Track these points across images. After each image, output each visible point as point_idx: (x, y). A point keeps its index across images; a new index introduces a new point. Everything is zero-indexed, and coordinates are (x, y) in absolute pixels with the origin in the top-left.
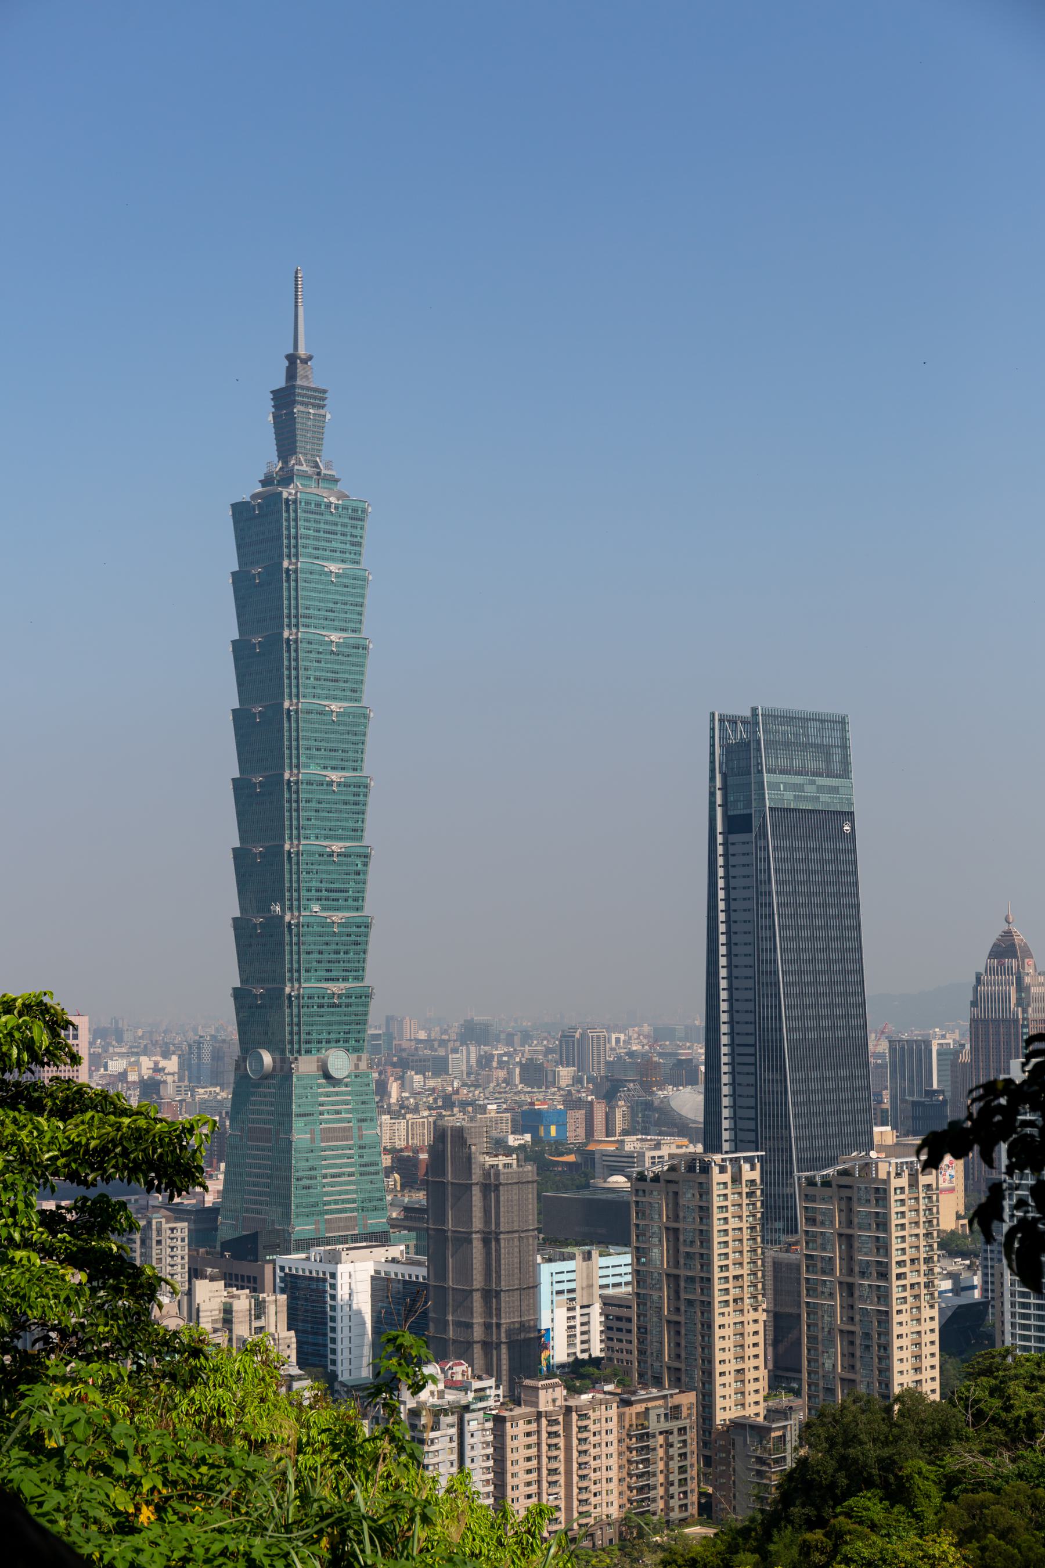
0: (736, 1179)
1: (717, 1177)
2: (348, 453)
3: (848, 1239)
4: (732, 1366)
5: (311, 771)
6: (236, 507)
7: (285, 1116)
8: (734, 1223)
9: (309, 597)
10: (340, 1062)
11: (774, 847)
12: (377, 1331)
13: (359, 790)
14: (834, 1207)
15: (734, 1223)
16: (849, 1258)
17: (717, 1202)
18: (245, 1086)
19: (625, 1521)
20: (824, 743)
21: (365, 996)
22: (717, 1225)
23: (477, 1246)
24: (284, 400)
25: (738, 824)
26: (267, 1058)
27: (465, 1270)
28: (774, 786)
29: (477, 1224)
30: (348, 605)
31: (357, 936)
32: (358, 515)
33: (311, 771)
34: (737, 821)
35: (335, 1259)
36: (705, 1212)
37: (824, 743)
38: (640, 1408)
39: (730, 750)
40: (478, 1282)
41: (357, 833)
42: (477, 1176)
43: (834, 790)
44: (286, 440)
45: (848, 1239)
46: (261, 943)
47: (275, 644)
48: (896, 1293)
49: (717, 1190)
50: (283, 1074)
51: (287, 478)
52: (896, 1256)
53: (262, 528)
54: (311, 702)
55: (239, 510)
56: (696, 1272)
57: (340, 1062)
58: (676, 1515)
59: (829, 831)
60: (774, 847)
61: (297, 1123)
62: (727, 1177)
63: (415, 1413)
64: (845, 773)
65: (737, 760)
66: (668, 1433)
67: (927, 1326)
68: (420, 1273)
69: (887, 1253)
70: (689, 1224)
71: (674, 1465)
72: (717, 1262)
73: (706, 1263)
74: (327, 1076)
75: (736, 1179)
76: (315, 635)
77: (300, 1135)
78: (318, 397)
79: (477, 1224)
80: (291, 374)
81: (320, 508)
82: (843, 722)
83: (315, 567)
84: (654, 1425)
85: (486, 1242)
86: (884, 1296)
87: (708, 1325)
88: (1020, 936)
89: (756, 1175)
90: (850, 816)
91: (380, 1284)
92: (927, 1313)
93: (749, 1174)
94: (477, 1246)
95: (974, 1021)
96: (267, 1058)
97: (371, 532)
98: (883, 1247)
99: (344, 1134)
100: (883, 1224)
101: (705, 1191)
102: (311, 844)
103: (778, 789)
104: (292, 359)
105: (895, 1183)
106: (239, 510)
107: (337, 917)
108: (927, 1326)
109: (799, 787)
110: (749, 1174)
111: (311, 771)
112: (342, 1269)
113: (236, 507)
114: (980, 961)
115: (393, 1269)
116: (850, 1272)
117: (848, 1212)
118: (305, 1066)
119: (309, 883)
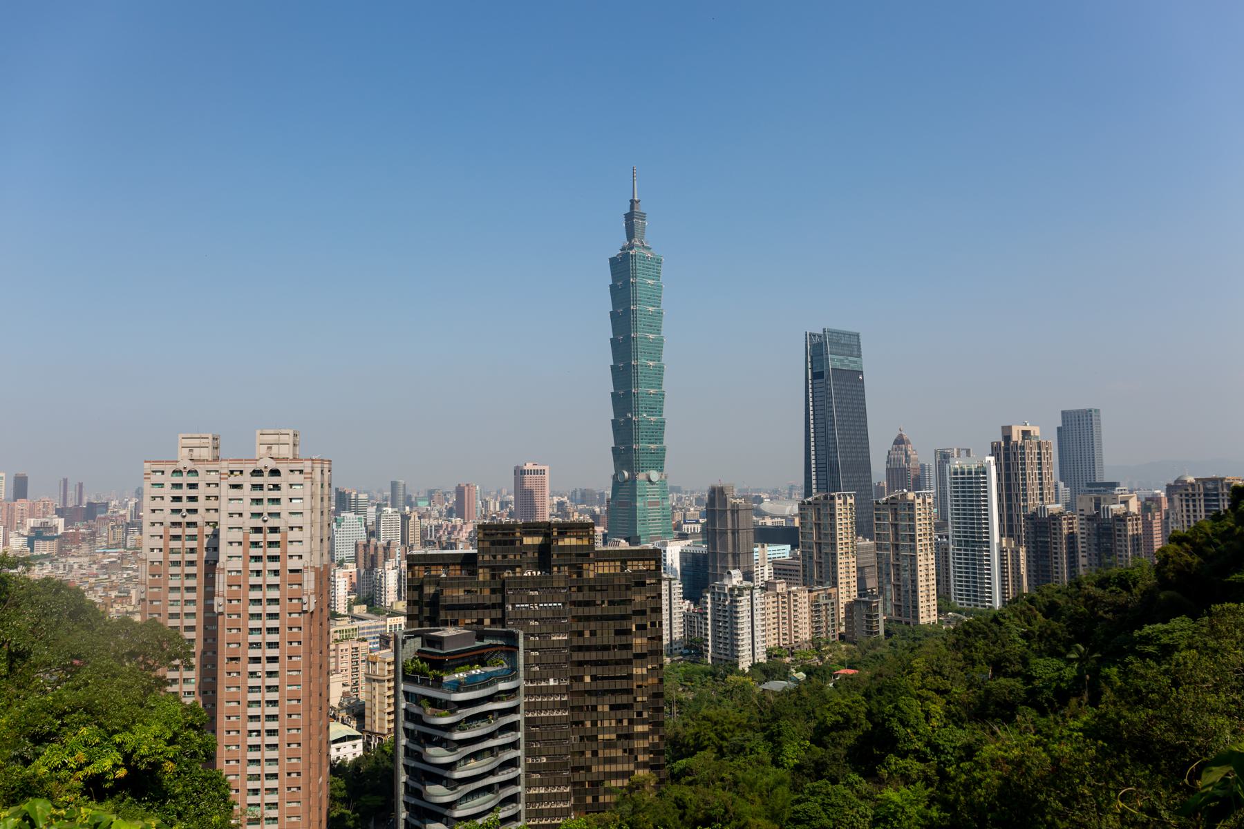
0: (845, 502)
1: (838, 501)
2: (653, 238)
3: (895, 526)
4: (844, 581)
5: (642, 361)
6: (611, 260)
7: (633, 497)
8: (844, 521)
9: (641, 293)
10: (654, 475)
11: (832, 385)
12: (682, 574)
13: (661, 368)
14: (889, 513)
15: (844, 521)
16: (896, 534)
17: (838, 512)
18: (617, 485)
19: (812, 641)
20: (851, 343)
21: (664, 450)
22: (838, 522)
23: (730, 535)
24: (629, 217)
25: (818, 375)
26: (626, 474)
27: (725, 546)
28: (833, 360)
29: (730, 526)
30: (655, 298)
31: (661, 426)
32: (659, 262)
33: (642, 361)
34: (817, 374)
35: (665, 545)
36: (833, 516)
37: (851, 343)
38: (815, 594)
39: (813, 346)
40: (730, 550)
41: (660, 385)
42: (729, 507)
43: (855, 362)
44: (630, 233)
45: (895, 526)
46: (624, 430)
47: (628, 311)
48: (919, 548)
49: (838, 507)
50: (633, 480)
51: (631, 247)
52: (918, 532)
53: (622, 267)
54: (643, 334)
55: (613, 261)
56: (829, 541)
57: (654, 475)
58: (831, 639)
59: (853, 379)
60: (832, 385)
61: (639, 499)
62: (841, 501)
63: (732, 590)
64: (859, 356)
65: (817, 349)
66: (826, 605)
67: (930, 562)
68: (703, 548)
69: (914, 530)
70: (825, 521)
71: (830, 618)
72: (839, 537)
73: (833, 537)
74: (650, 481)
75: (845, 502)
76: (643, 308)
77: (639, 504)
78: (643, 216)
79: (730, 526)
80: (632, 207)
81: (645, 258)
82: (858, 335)
83: (643, 281)
84: (822, 601)
85: (733, 533)
86: (913, 549)
87: (835, 563)
88: (906, 436)
89: (852, 501)
90: (861, 373)
91: (683, 555)
92: (931, 556)
93: (850, 501)
94: (730, 535)
95: (888, 469)
96: (626, 474)
97: (664, 269)
98: (912, 528)
99: (656, 504)
100: (912, 518)
101: (833, 507)
102: (643, 389)
103: (835, 361)
104: (632, 201)
105: (917, 501)
106: (613, 261)
107: (652, 418)
108: (930, 562)
109: (841, 361)
110: (850, 501)
111: (642, 361)
112: (668, 549)
113: (611, 260)
114: (890, 446)
115: (689, 549)
116: (897, 539)
117: (896, 514)
118: (641, 476)
119: (642, 405)
